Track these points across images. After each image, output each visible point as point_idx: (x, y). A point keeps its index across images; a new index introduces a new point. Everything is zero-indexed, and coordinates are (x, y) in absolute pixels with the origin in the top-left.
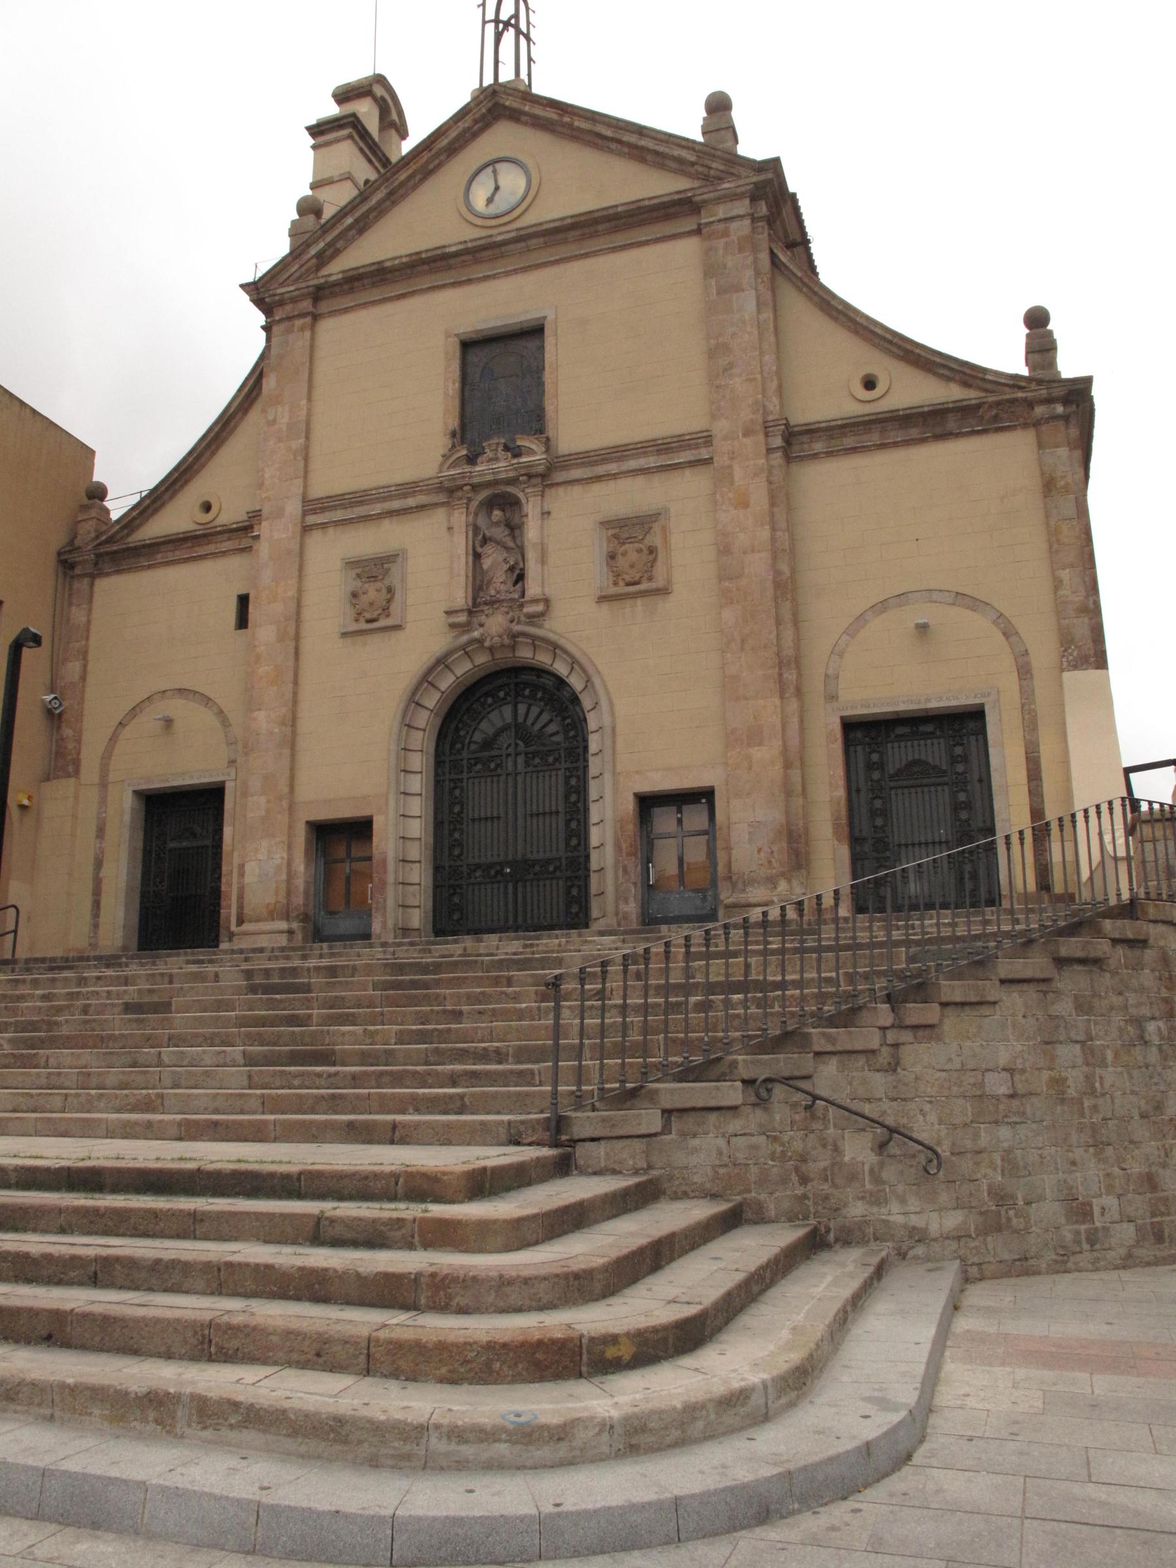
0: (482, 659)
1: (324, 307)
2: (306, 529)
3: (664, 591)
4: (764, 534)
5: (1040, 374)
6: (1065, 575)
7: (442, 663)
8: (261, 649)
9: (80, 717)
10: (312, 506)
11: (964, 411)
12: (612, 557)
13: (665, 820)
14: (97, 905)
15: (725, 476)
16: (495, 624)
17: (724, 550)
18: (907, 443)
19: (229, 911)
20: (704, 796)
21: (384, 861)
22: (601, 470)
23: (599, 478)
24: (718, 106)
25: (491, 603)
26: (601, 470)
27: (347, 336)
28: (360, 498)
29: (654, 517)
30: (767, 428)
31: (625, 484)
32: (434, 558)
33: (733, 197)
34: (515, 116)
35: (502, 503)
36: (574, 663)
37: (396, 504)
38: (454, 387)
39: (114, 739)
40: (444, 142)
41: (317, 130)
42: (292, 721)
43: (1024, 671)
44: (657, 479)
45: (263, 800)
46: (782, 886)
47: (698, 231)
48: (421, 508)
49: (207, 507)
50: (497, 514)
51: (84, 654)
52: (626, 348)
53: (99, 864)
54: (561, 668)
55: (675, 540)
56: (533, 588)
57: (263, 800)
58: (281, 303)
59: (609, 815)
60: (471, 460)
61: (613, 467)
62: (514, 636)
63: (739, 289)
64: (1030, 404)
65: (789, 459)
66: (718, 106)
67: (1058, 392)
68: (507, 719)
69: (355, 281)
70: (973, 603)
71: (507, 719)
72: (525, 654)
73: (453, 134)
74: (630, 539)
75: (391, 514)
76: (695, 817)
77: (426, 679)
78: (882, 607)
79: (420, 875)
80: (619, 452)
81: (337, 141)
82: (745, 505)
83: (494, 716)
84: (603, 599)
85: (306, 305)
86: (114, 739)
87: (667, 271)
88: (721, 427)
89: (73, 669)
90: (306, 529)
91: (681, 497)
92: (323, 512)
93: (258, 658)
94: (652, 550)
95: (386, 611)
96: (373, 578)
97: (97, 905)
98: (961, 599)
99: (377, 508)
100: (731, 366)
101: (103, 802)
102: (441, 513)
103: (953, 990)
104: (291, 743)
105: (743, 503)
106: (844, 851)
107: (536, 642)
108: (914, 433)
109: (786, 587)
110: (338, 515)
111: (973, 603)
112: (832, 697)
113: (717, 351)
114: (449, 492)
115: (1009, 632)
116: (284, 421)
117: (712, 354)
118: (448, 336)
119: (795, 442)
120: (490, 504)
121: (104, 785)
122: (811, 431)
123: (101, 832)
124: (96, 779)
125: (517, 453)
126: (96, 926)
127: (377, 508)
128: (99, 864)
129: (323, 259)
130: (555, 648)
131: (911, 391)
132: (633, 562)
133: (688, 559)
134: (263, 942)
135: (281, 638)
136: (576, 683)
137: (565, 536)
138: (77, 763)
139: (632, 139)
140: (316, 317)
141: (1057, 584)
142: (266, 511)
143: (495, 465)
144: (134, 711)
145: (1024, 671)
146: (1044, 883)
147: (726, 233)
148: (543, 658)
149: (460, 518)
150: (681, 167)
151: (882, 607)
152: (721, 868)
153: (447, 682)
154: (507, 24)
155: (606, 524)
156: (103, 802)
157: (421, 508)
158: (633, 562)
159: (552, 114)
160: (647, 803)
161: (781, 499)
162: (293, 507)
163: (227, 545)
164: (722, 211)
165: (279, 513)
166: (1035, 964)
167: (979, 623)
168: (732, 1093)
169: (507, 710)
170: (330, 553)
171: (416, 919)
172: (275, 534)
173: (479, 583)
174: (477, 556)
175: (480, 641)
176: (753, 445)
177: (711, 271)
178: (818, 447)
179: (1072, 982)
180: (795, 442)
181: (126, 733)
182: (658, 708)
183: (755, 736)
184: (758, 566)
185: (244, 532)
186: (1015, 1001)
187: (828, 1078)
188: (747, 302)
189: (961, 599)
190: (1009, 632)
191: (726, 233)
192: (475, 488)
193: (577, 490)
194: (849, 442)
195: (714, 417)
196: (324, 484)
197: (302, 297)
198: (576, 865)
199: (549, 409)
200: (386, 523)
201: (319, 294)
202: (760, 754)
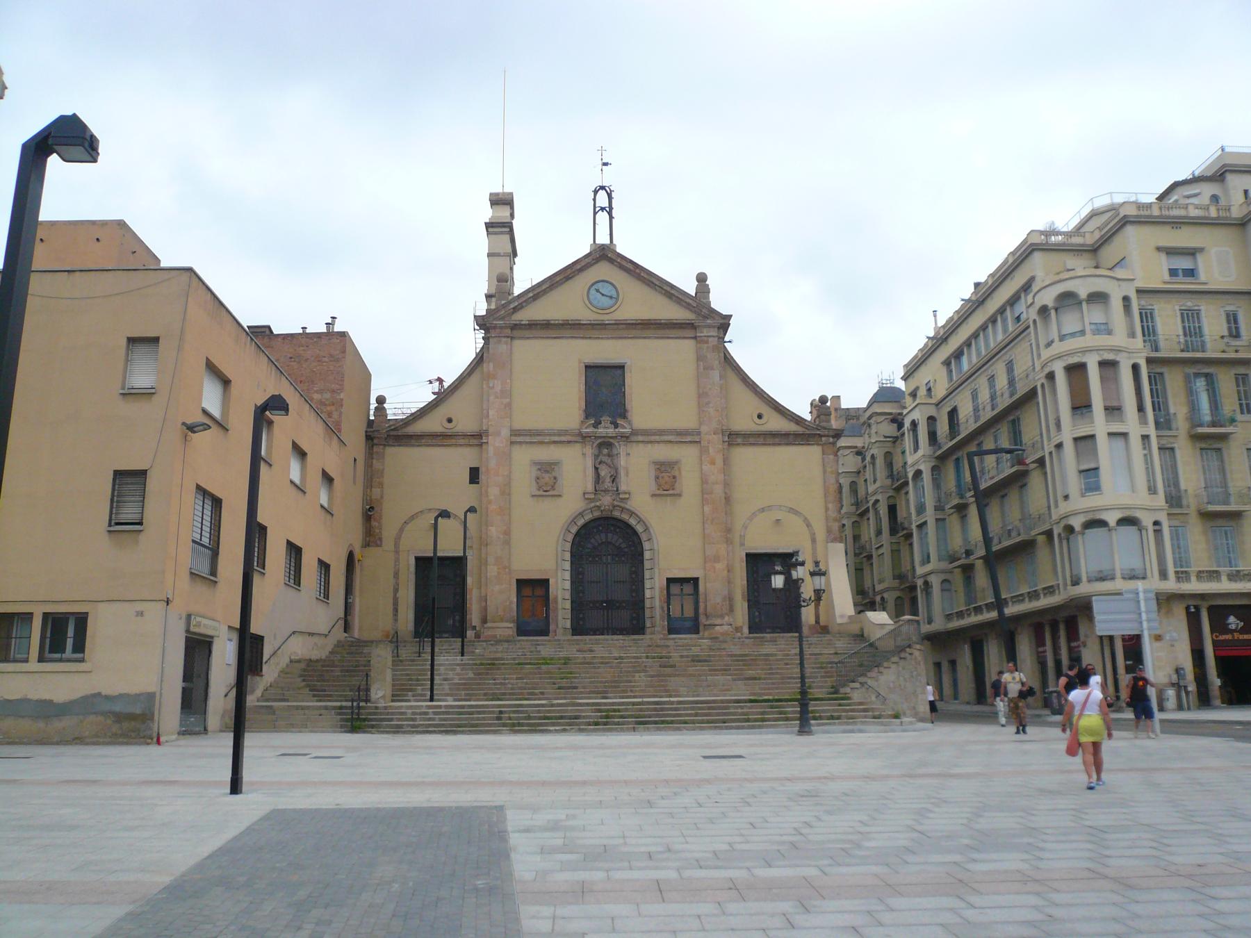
0: (597, 514)
1: (516, 333)
2: (512, 443)
3: (680, 495)
4: (721, 477)
5: (824, 424)
6: (830, 506)
7: (581, 514)
8: (492, 498)
9: (381, 517)
10: (515, 433)
11: (796, 435)
12: (657, 478)
13: (675, 589)
14: (396, 610)
15: (704, 451)
16: (606, 500)
17: (704, 481)
18: (774, 444)
19: (474, 617)
20: (695, 581)
21: (556, 598)
22: (653, 438)
23: (651, 442)
24: (702, 278)
25: (606, 491)
26: (653, 438)
27: (527, 351)
28: (538, 433)
29: (676, 463)
30: (723, 432)
31: (662, 446)
32: (576, 468)
33: (709, 326)
34: (611, 261)
35: (605, 445)
36: (640, 521)
37: (556, 439)
38: (583, 387)
39: (401, 530)
40: (578, 267)
41: (489, 226)
42: (507, 533)
43: (814, 541)
44: (676, 447)
45: (495, 568)
46: (726, 618)
47: (695, 338)
48: (569, 442)
49: (450, 421)
50: (605, 451)
51: (381, 485)
52: (660, 383)
53: (396, 590)
54: (632, 522)
55: (683, 473)
56: (623, 488)
57: (495, 568)
58: (495, 328)
59: (657, 586)
60: (596, 425)
61: (657, 438)
62: (614, 506)
63: (712, 369)
64: (820, 436)
65: (730, 445)
66: (702, 278)
67: (831, 433)
68: (607, 543)
69: (532, 325)
70: (796, 512)
71: (607, 543)
72: (617, 514)
73: (583, 264)
74: (666, 471)
75: (555, 442)
76: (688, 589)
77: (573, 521)
78: (763, 510)
79: (568, 605)
80: (661, 432)
81: (502, 233)
82: (713, 463)
83: (597, 537)
84: (653, 495)
85: (508, 331)
86: (401, 530)
87: (681, 351)
88: (704, 429)
89: (376, 492)
90: (512, 443)
91: (686, 456)
92: (521, 437)
93: (490, 502)
94: (674, 477)
95: (553, 488)
96: (547, 472)
97: (396, 610)
98: (792, 511)
99: (547, 439)
100: (708, 403)
101: (397, 560)
102: (578, 446)
103: (885, 664)
104: (507, 542)
105: (713, 463)
106: (746, 604)
107: (623, 509)
108: (777, 440)
109: (728, 499)
110: (528, 439)
111: (796, 512)
112: (742, 544)
113: (701, 395)
114: (584, 438)
115: (808, 525)
116: (498, 388)
117: (700, 396)
118: (580, 362)
119: (734, 438)
120: (600, 446)
121: (397, 552)
122: (737, 434)
123: (396, 575)
124: (392, 548)
125: (616, 426)
126: (396, 620)
127: (547, 439)
128: (396, 590)
129: (515, 310)
130: (632, 513)
131: (775, 423)
132: (666, 480)
133: (689, 482)
134: (499, 633)
135: (503, 493)
136: (639, 529)
137: (636, 465)
138: (380, 539)
139: (668, 289)
140: (512, 338)
141: (827, 509)
142: (491, 430)
143: (606, 430)
144: (412, 518)
145: (814, 541)
146: (817, 622)
147: (707, 342)
148: (625, 517)
149: (589, 451)
150: (688, 306)
151: (763, 510)
152: (701, 610)
153: (581, 522)
154: (603, 209)
155: (655, 463)
156: (397, 560)
157: (569, 442)
158: (666, 480)
159: (629, 266)
160: (670, 581)
161: (726, 461)
162: (505, 432)
163: (462, 441)
164: (705, 332)
165: (498, 434)
166: (895, 659)
167: (798, 521)
168: (856, 685)
169: (603, 536)
170: (524, 457)
171: (568, 624)
172: (496, 443)
173: (598, 478)
174: (596, 469)
175: (599, 507)
176: (717, 439)
177: (700, 358)
178: (739, 440)
179: (902, 663)
180: (734, 438)
181: (408, 527)
182: (676, 544)
183: (717, 559)
184: (719, 490)
185: (478, 438)
186: (893, 666)
187: (870, 682)
188: (716, 375)
189: (792, 511)
190: (808, 525)
191: (707, 342)
192: (596, 438)
193: (641, 445)
194: (752, 440)
195: (700, 424)
196: (522, 422)
197: (506, 327)
198: (637, 604)
199: (628, 406)
200: (552, 447)
201: (515, 327)
202: (719, 566)
